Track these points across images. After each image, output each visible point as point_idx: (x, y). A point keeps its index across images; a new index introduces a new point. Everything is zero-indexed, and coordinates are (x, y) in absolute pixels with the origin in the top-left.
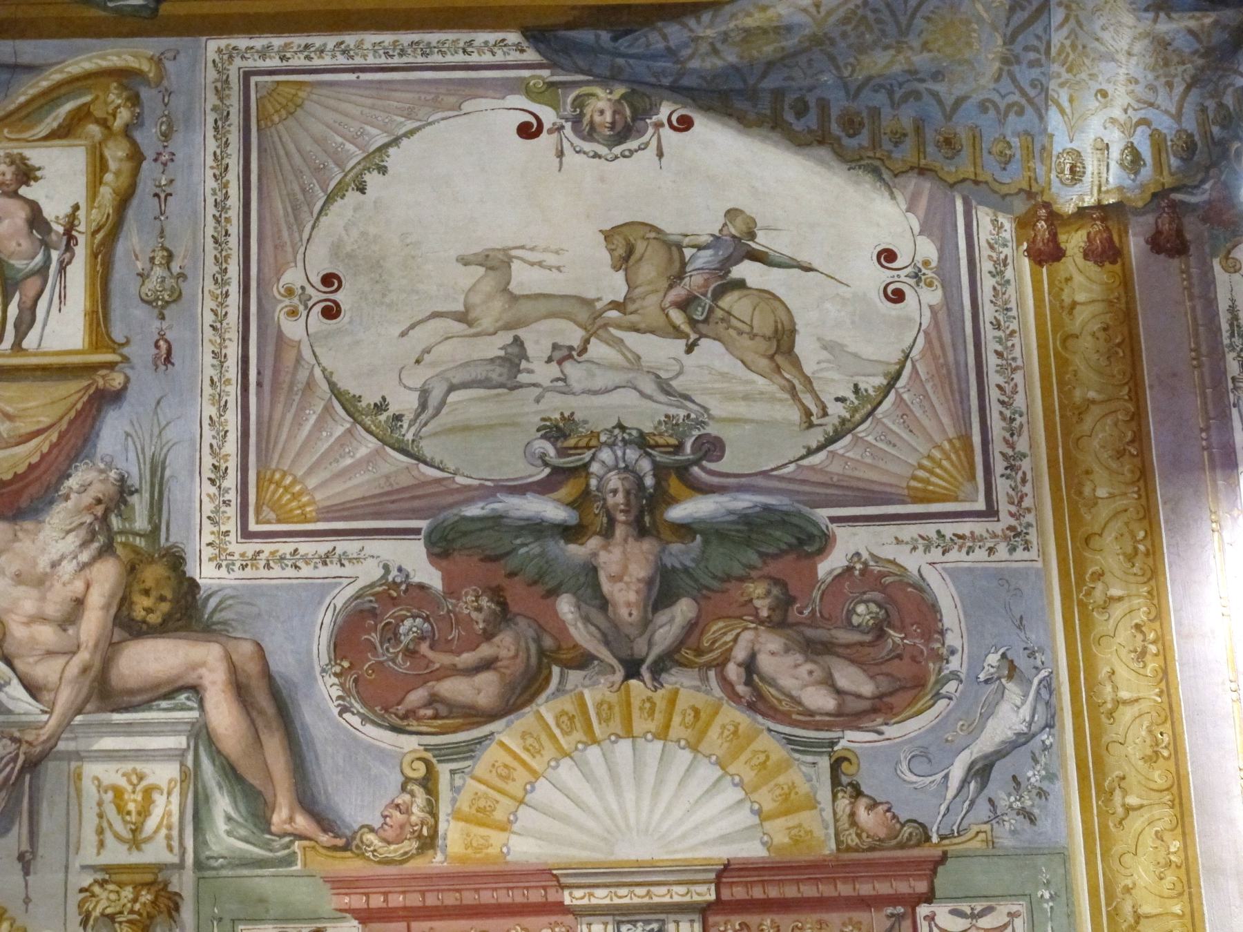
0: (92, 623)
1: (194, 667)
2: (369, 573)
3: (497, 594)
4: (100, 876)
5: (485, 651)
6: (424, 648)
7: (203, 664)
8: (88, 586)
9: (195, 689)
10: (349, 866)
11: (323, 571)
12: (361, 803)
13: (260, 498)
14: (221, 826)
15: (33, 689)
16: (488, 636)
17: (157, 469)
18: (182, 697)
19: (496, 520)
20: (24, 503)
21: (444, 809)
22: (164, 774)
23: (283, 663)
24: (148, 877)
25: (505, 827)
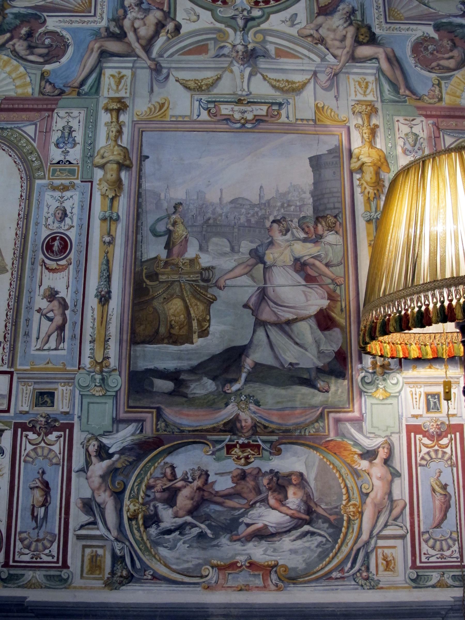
0: (349, 41)
1: (376, 53)
2: (419, 34)
3: (452, 40)
4: (357, 102)
5: (451, 54)
6: (435, 52)
7: (379, 53)
8: (347, 32)
9: (377, 59)
10: (420, 104)
11: (407, 32)
12: (422, 90)
13: (390, 14)
14: (387, 92)
15: (335, 56)
16: (451, 51)
17: (362, 5)
18: (374, 61)
19: (450, 23)
20: (328, 11)
21: (444, 92)
22: (371, 79)
23: (398, 54)
24: (369, 104)
25: (459, 97)
